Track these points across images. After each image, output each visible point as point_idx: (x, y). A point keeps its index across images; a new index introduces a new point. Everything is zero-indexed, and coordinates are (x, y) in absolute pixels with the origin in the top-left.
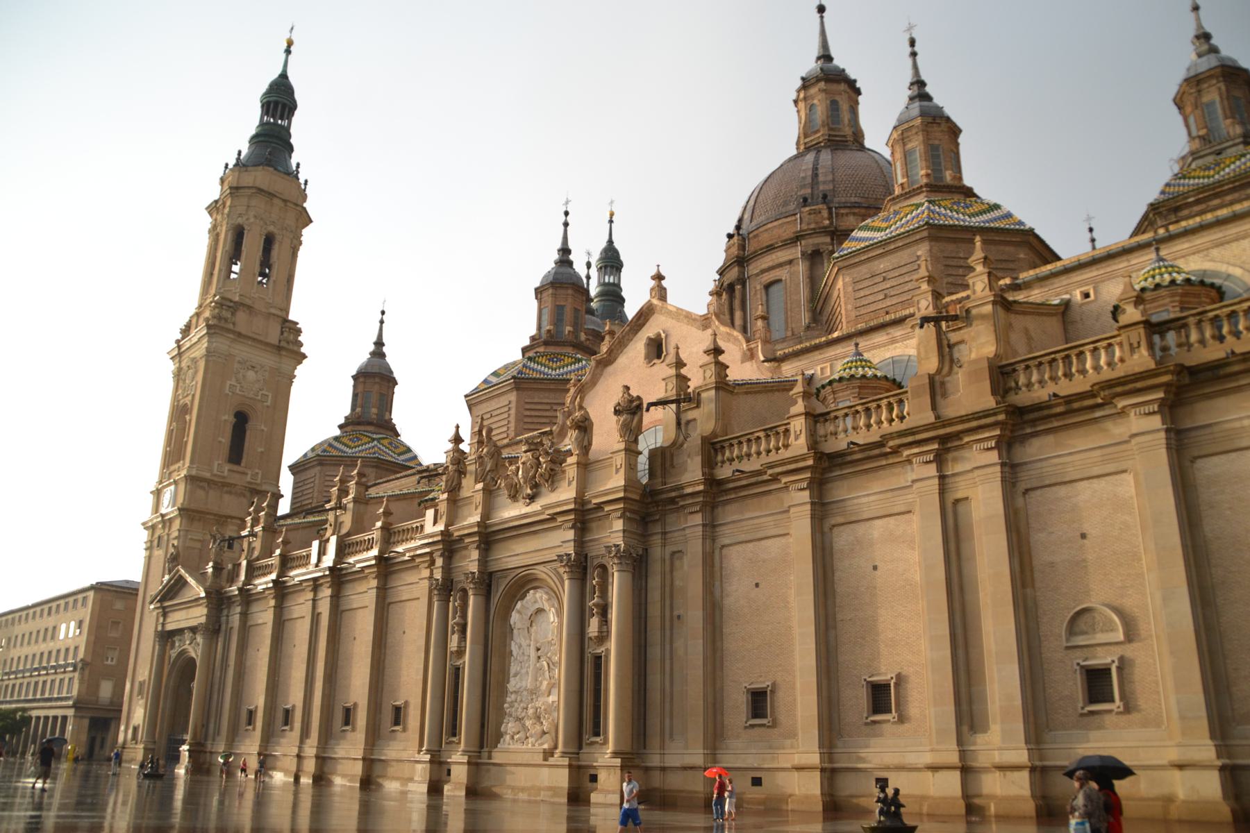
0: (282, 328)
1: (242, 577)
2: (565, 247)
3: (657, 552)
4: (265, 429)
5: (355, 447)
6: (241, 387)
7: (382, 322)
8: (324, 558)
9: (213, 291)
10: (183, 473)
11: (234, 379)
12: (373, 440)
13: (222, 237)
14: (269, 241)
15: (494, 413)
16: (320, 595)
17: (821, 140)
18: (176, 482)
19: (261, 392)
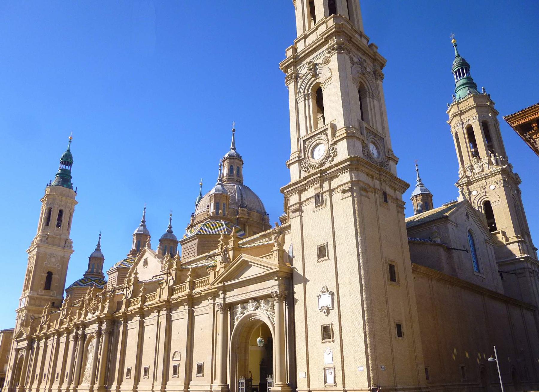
0: (65, 242)
1: (38, 331)
2: (143, 220)
3: (115, 330)
4: (58, 277)
5: (85, 284)
6: (49, 264)
7: (100, 238)
8: (57, 326)
9: (41, 231)
10: (28, 294)
11: (47, 261)
12: (92, 280)
13: (44, 211)
14: (61, 212)
15: (113, 278)
16: (55, 338)
17: (226, 180)
18: (26, 297)
19: (57, 265)
